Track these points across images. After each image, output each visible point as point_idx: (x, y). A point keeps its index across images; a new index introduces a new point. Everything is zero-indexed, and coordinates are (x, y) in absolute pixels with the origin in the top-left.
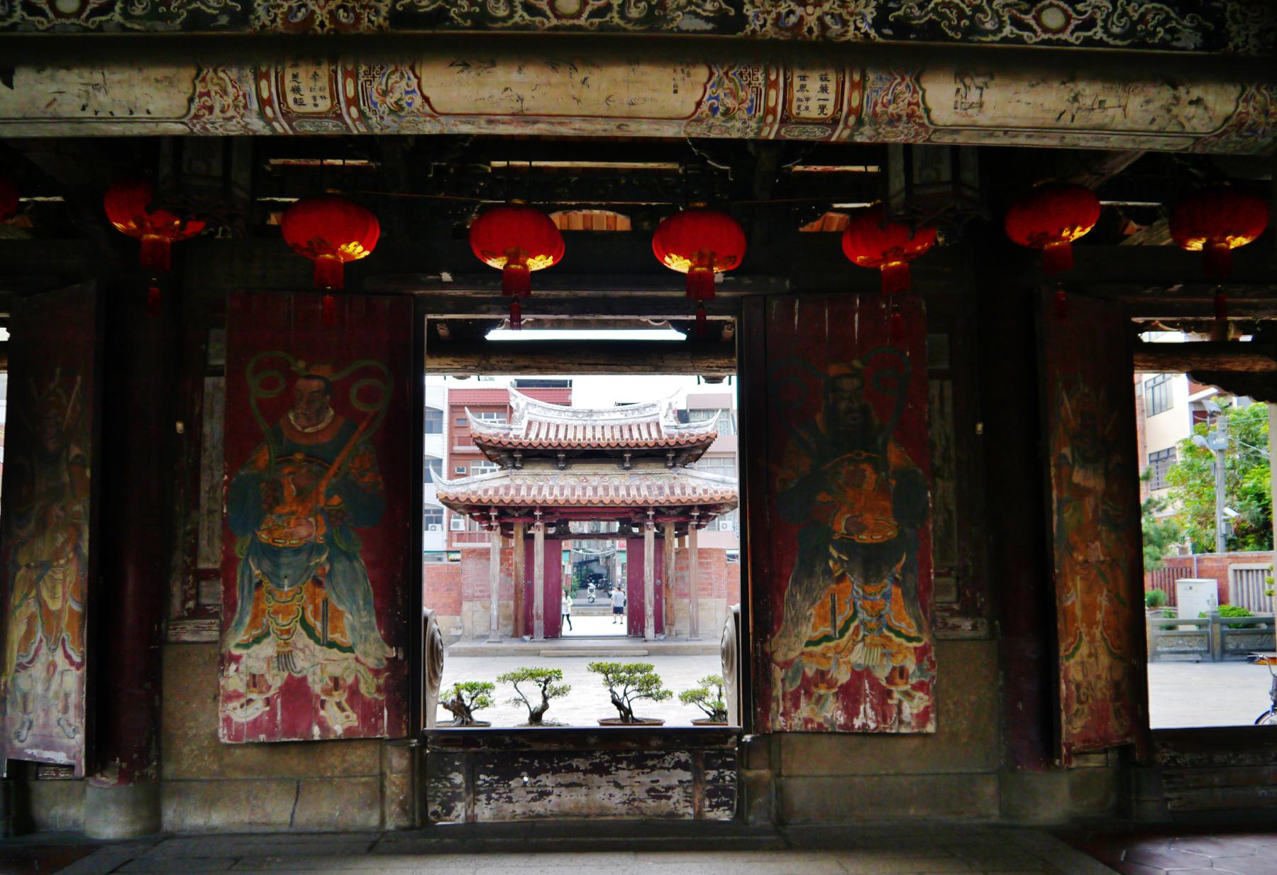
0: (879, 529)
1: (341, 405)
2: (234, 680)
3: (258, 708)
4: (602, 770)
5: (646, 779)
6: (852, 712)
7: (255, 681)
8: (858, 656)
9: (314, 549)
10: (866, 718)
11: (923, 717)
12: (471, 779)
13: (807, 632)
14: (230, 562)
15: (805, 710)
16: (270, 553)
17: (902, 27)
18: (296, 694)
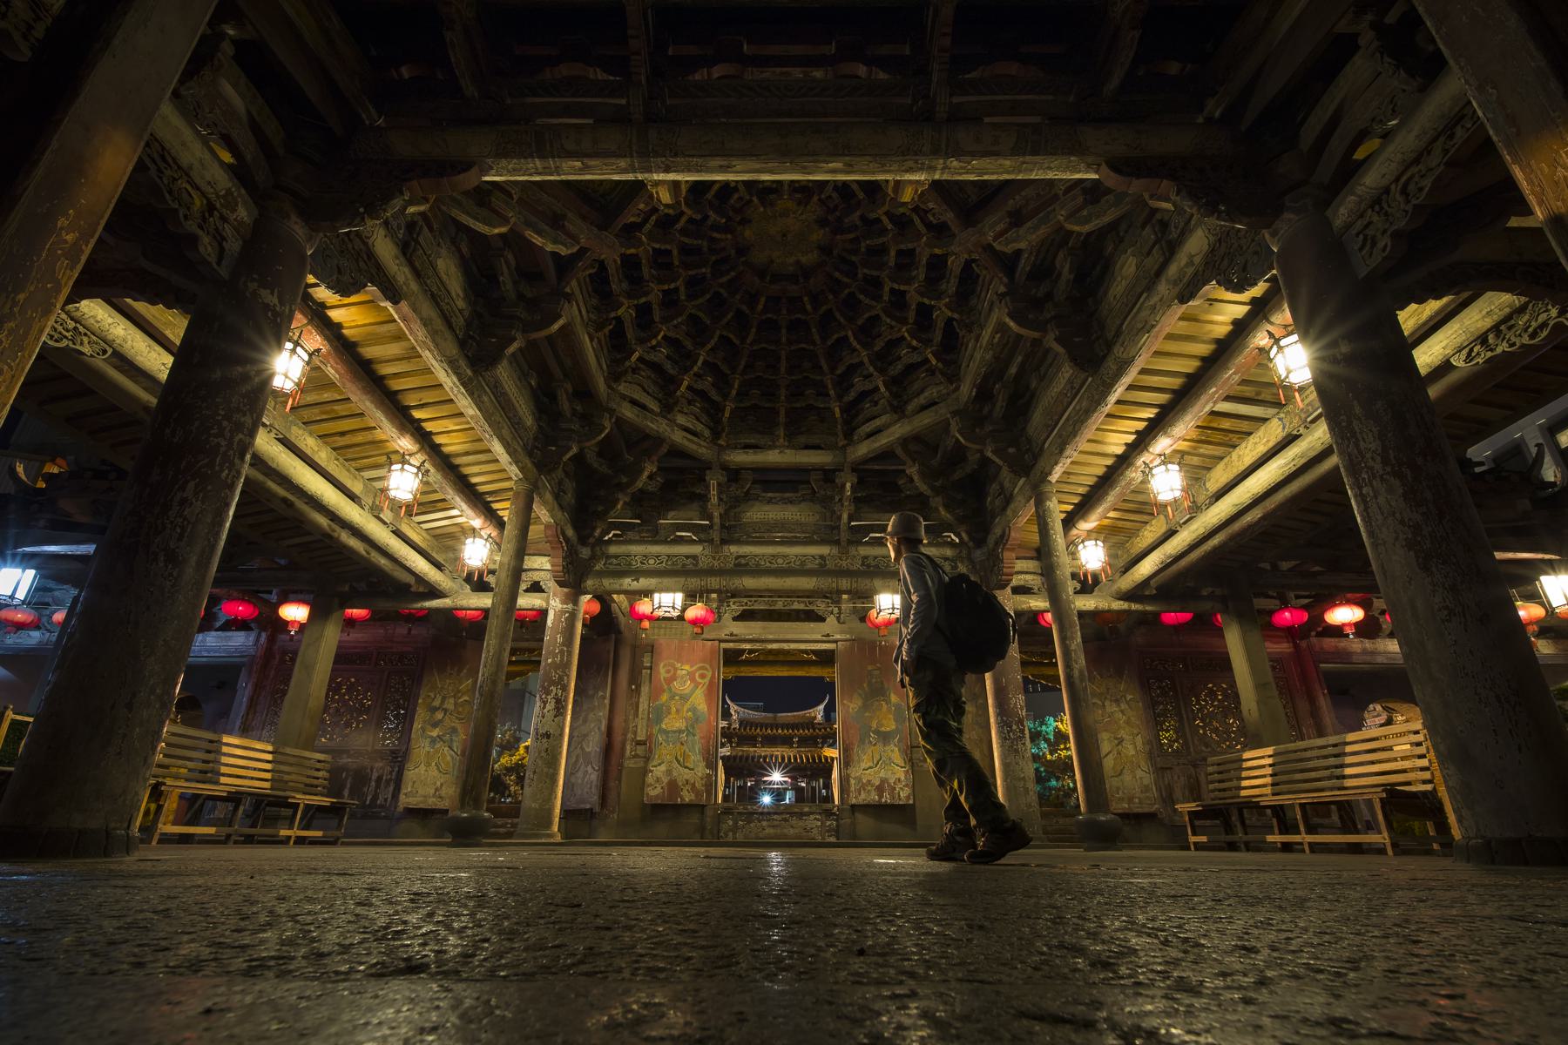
0: (890, 725)
1: (693, 679)
2: (650, 779)
3: (658, 791)
4: (785, 820)
5: (801, 823)
6: (881, 796)
7: (658, 780)
8: (882, 774)
9: (680, 731)
10: (886, 799)
11: (908, 797)
12: (736, 823)
13: (863, 765)
14: (649, 737)
15: (863, 795)
16: (666, 732)
17: (869, 566)
18: (673, 786)
